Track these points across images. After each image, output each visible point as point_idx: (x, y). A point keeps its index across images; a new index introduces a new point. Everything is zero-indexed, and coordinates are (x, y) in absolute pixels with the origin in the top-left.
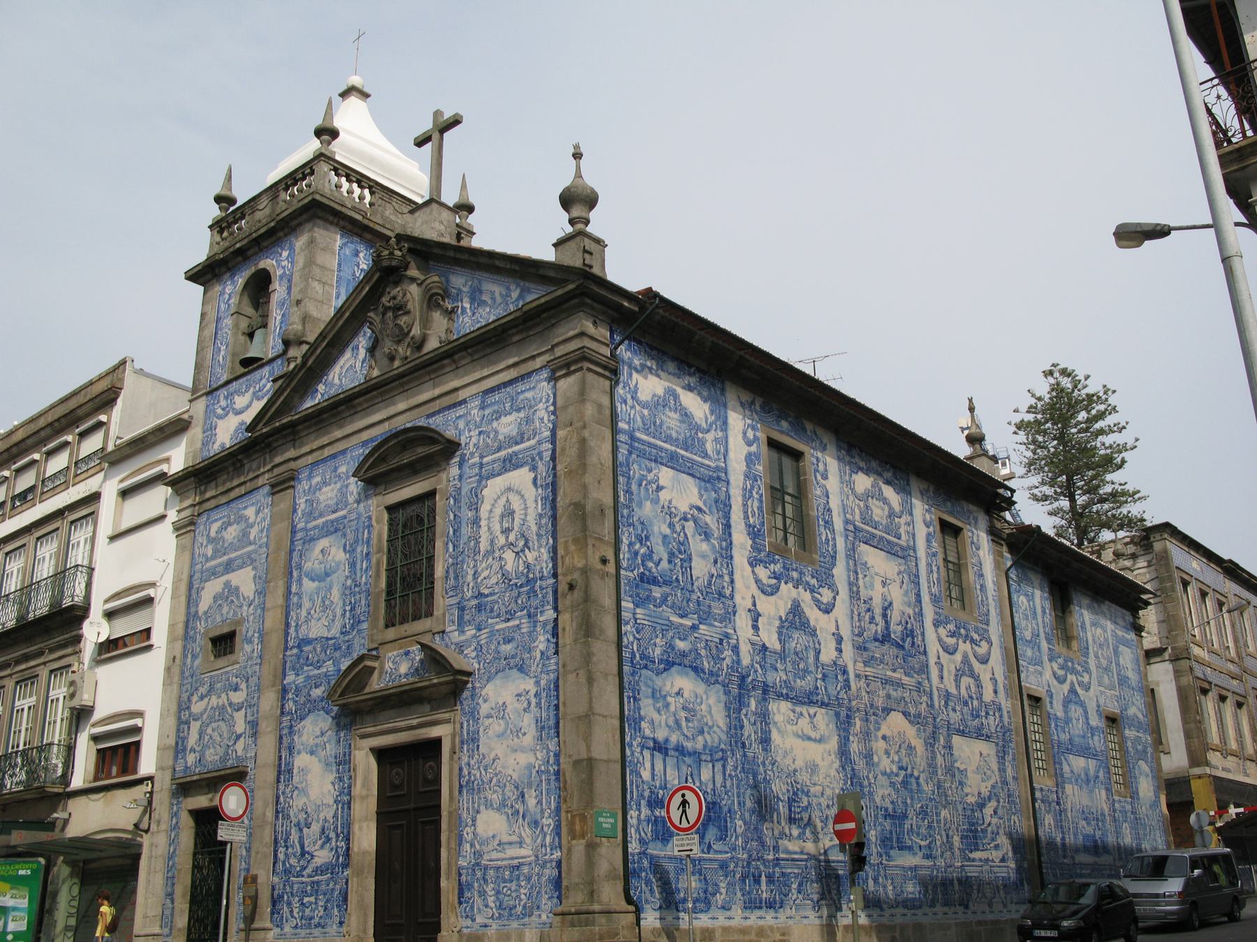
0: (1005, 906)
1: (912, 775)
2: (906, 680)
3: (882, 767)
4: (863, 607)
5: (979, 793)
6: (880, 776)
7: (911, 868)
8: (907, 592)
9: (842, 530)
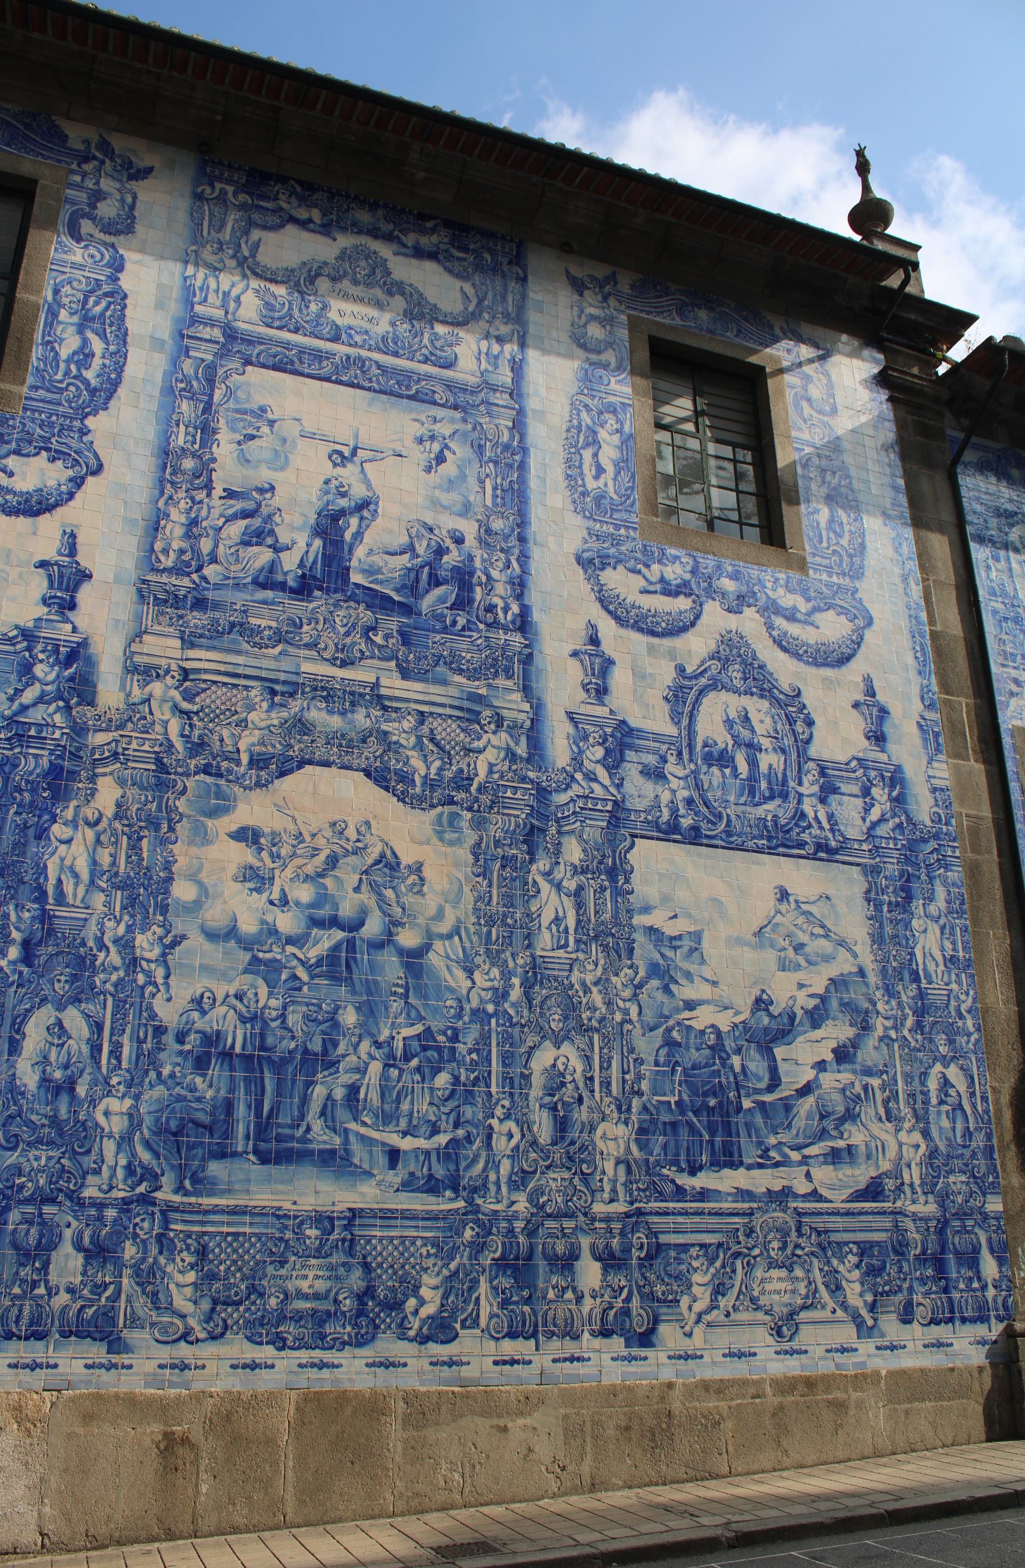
0: (864, 1330)
1: (385, 942)
2: (393, 684)
3: (215, 915)
4: (216, 507)
5: (761, 1004)
6: (195, 941)
7: (324, 1220)
8: (450, 484)
9: (166, 332)
